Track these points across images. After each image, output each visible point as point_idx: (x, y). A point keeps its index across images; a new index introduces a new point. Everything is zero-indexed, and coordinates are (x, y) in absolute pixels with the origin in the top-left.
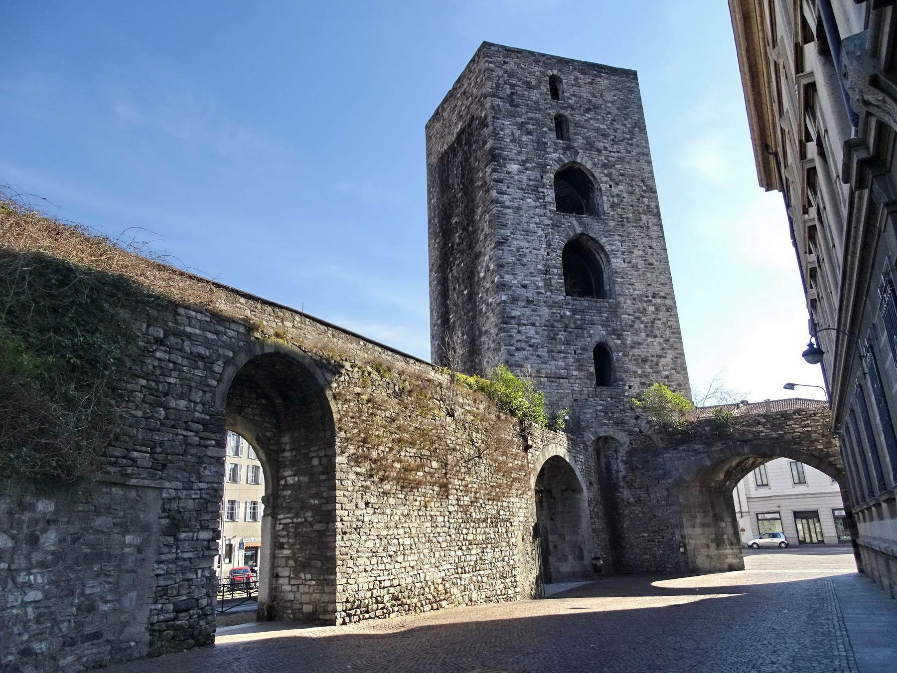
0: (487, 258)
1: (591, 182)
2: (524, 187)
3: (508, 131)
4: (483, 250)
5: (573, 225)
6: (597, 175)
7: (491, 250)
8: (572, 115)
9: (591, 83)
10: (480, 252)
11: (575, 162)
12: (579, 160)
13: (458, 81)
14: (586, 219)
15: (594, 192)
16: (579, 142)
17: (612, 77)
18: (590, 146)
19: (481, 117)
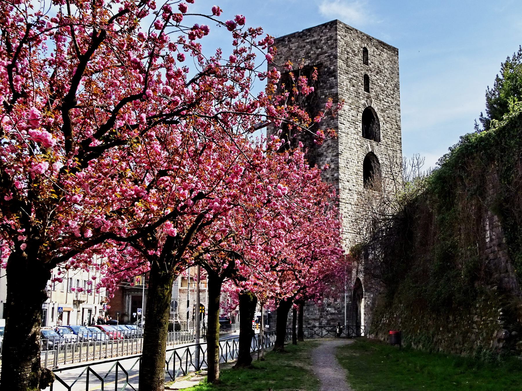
0: (328, 159)
1: (374, 119)
2: (350, 120)
3: (345, 83)
4: (325, 153)
5: (368, 144)
6: (378, 116)
7: (333, 156)
8: (371, 75)
9: (379, 55)
10: (323, 154)
11: (370, 107)
12: (372, 106)
13: (309, 30)
14: (374, 144)
15: (373, 124)
16: (373, 94)
17: (388, 52)
18: (377, 97)
19: (330, 69)
